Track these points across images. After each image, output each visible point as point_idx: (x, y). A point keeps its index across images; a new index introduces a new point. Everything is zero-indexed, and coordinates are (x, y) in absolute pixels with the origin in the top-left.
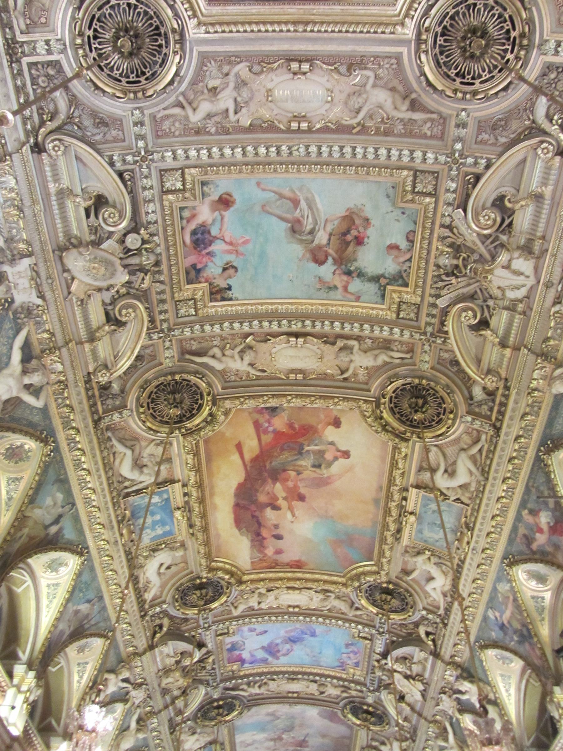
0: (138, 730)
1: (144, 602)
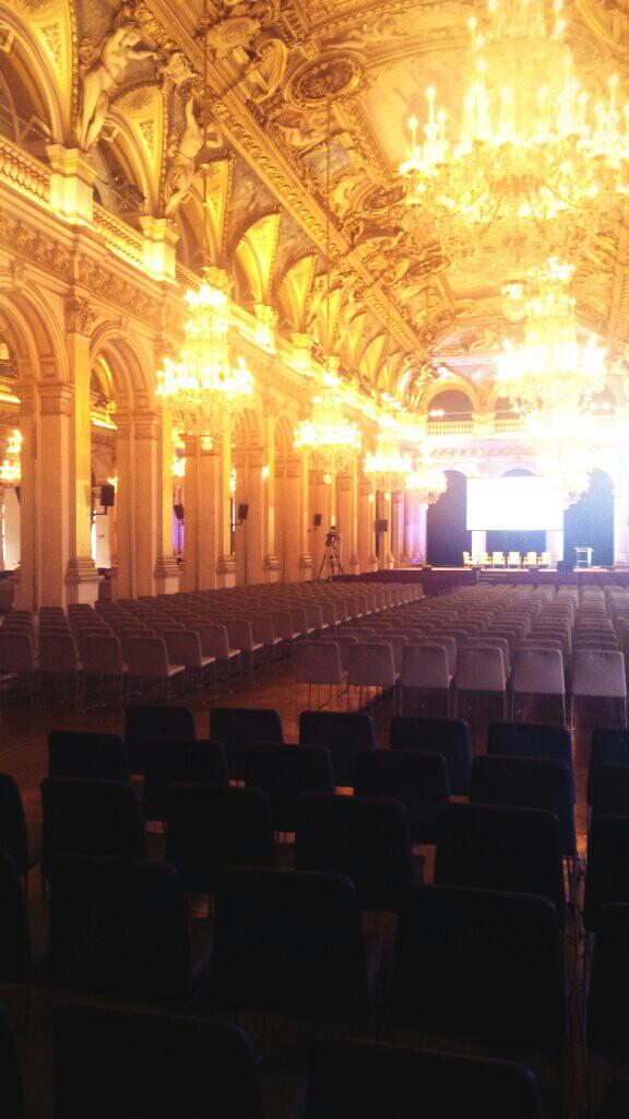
0: (356, 301)
1: (338, 219)
